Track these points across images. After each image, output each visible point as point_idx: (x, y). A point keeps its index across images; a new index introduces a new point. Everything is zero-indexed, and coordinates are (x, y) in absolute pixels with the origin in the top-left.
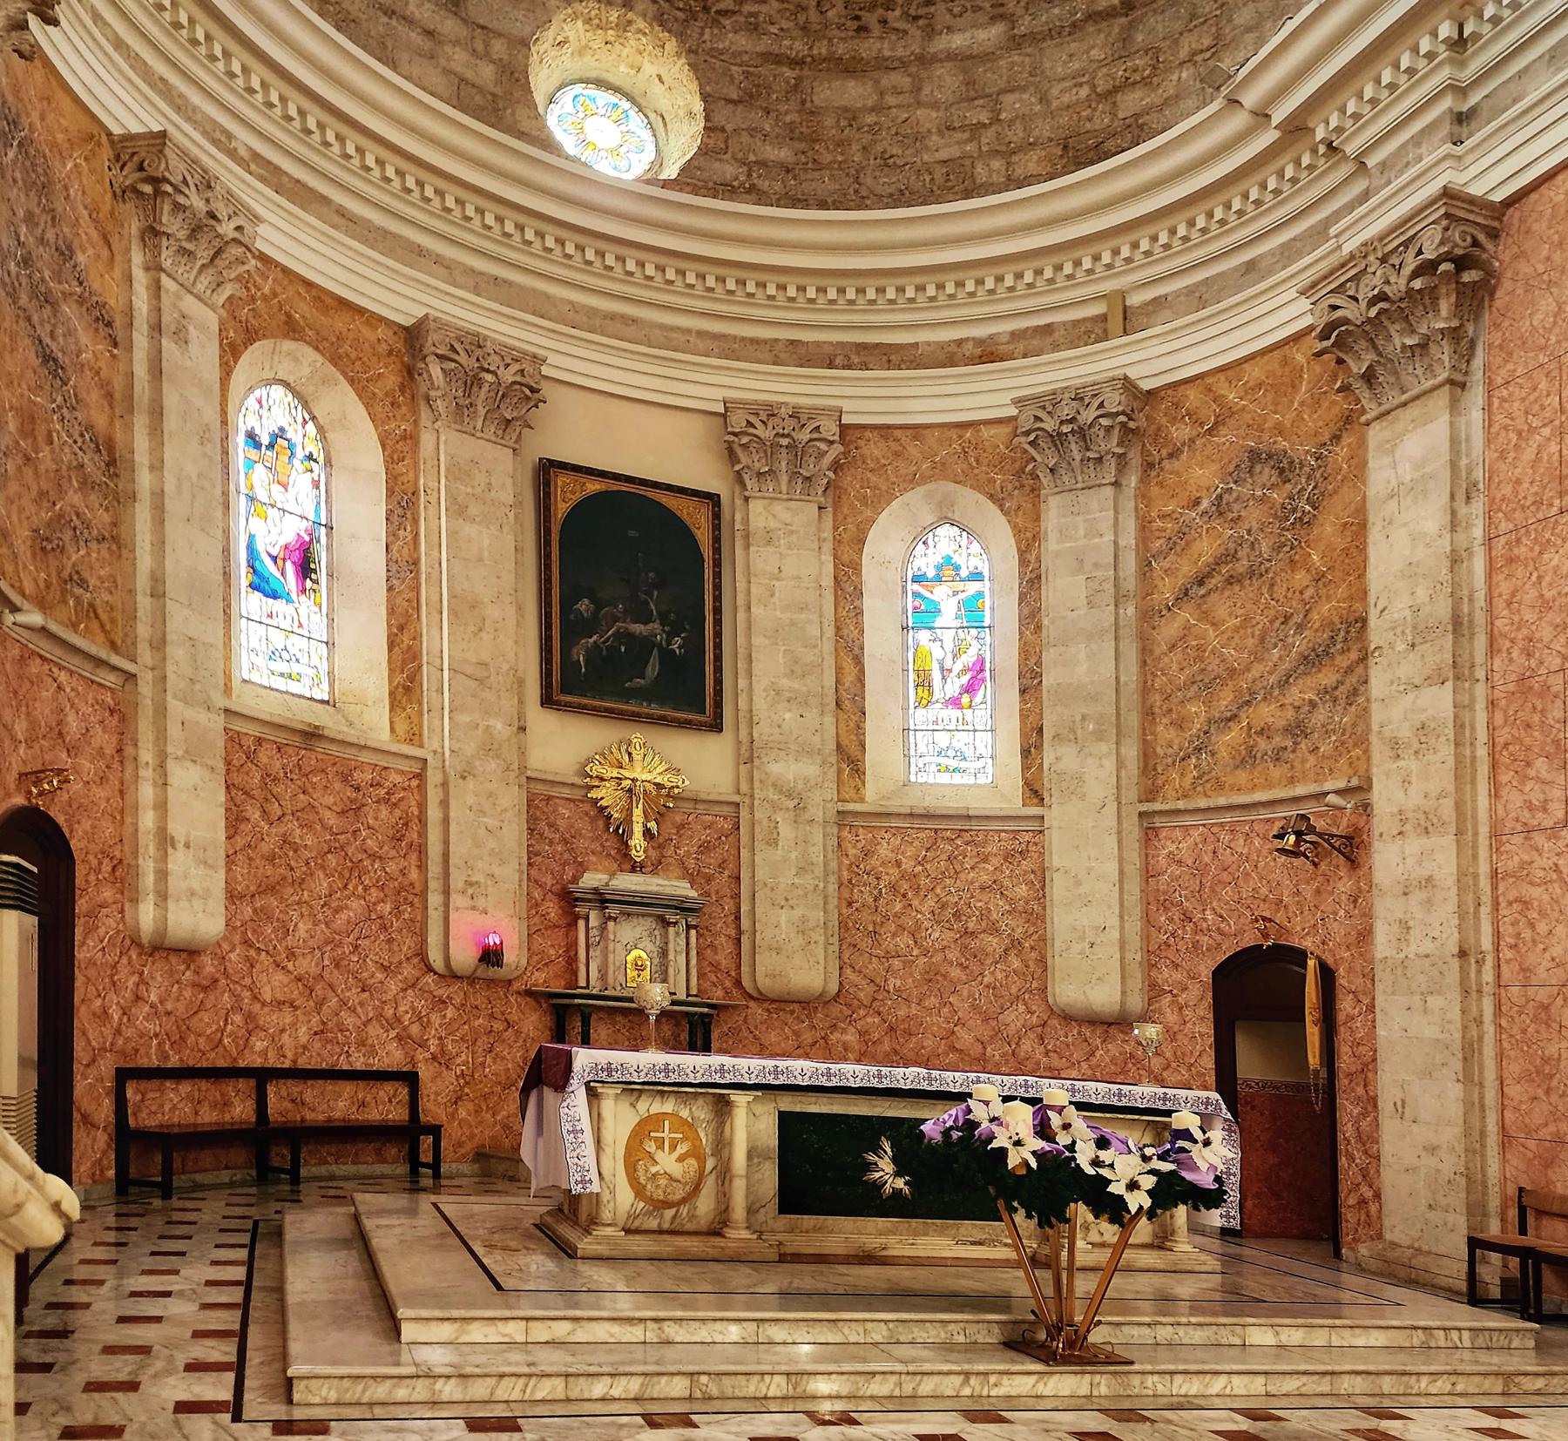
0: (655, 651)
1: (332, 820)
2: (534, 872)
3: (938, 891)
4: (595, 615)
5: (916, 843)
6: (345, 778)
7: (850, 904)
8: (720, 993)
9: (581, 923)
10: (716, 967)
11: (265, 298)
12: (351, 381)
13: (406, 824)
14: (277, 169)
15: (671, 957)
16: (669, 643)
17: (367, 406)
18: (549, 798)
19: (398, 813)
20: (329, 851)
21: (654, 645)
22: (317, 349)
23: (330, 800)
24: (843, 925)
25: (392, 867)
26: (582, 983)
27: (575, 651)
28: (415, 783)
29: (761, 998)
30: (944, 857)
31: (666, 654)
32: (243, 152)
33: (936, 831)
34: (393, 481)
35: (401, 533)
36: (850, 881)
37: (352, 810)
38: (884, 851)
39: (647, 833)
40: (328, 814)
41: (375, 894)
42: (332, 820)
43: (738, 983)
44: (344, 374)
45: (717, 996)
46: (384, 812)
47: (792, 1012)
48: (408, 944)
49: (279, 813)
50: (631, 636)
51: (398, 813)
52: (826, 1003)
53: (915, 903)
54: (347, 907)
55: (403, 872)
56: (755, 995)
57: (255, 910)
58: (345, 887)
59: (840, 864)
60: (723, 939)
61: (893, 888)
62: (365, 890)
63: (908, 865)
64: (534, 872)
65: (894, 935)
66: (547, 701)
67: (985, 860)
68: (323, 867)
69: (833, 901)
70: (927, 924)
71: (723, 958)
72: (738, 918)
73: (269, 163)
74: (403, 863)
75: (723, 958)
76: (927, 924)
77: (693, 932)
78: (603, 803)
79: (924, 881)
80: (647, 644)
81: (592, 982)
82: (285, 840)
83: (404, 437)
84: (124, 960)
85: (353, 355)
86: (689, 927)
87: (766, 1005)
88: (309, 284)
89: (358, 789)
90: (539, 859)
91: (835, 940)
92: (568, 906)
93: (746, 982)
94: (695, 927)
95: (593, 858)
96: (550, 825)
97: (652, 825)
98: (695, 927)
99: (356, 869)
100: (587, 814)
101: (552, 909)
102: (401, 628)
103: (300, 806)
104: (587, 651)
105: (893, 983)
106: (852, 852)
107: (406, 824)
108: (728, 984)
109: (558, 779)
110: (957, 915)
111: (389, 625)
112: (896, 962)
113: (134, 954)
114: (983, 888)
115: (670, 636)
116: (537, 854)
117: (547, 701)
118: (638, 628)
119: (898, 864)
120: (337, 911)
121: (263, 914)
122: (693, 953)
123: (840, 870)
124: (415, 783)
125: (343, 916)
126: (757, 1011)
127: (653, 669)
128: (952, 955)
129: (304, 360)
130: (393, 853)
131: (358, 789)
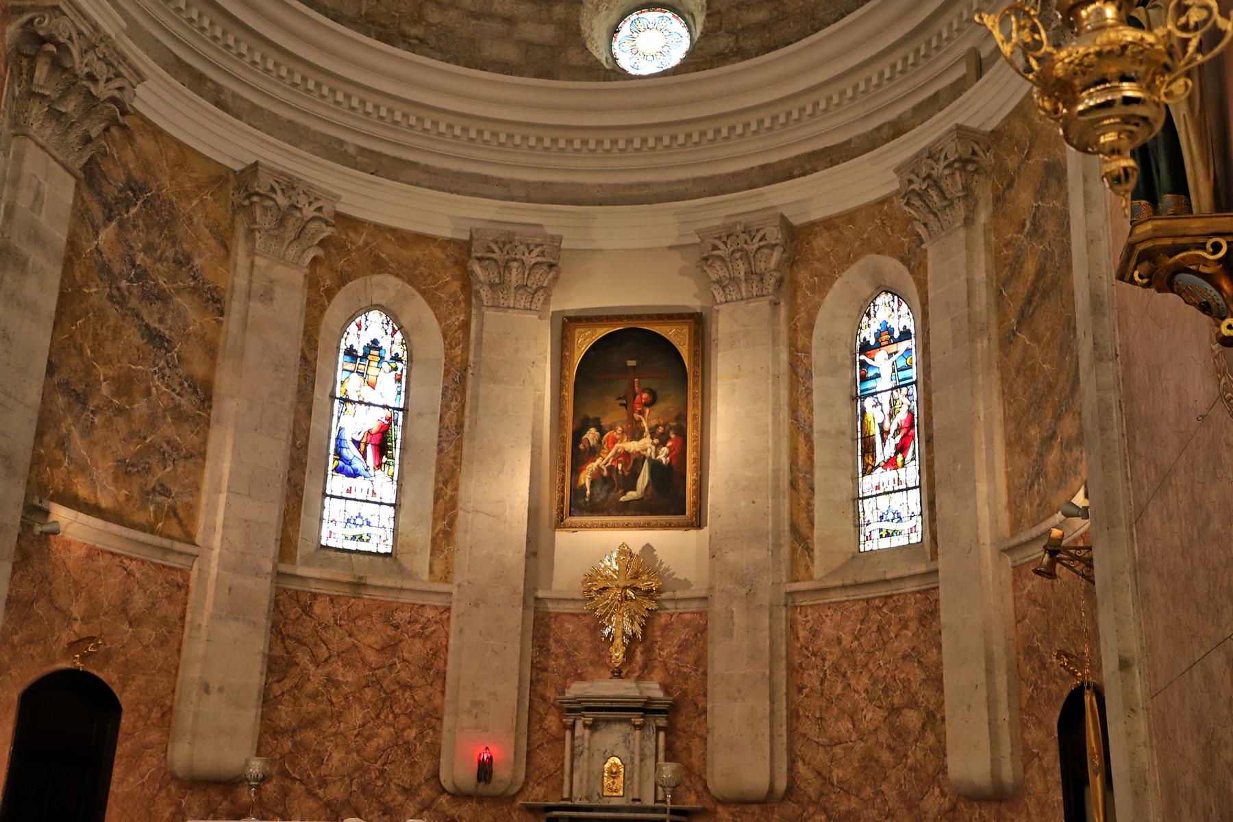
0: (646, 463)
1: (372, 657)
3: (871, 666)
4: (600, 442)
5: (853, 617)
6: (387, 620)
7: (800, 690)
11: (359, 249)
12: (423, 293)
13: (435, 654)
14: (380, 154)
16: (657, 455)
17: (434, 309)
19: (429, 644)
20: (367, 686)
21: (645, 457)
22: (397, 276)
23: (371, 639)
27: (582, 475)
28: (445, 616)
30: (875, 628)
31: (656, 466)
32: (351, 150)
33: (867, 601)
34: (449, 359)
35: (453, 404)
37: (390, 647)
38: (828, 629)
40: (369, 651)
41: (403, 720)
42: (372, 657)
44: (418, 290)
46: (418, 643)
48: (426, 766)
49: (326, 655)
50: (626, 454)
51: (429, 644)
53: (853, 682)
54: (377, 735)
57: (294, 744)
58: (378, 716)
61: (836, 667)
62: (395, 717)
63: (847, 639)
67: (905, 627)
68: (360, 700)
70: (862, 705)
73: (372, 151)
74: (430, 690)
76: (862, 705)
79: (860, 657)
80: (639, 459)
82: (331, 681)
83: (460, 327)
84: (163, 794)
85: (426, 272)
88: (394, 231)
89: (397, 627)
96: (556, 641)
99: (388, 699)
102: (446, 483)
103: (344, 648)
104: (593, 474)
105: (837, 774)
106: (802, 634)
107: (435, 654)
109: (561, 596)
110: (885, 691)
111: (437, 481)
112: (838, 750)
113: (173, 788)
114: (904, 657)
115: (657, 446)
118: (633, 446)
119: (839, 640)
120: (368, 740)
121: (299, 747)
125: (373, 744)
127: (644, 479)
128: (883, 736)
129: (389, 285)
130: (422, 682)
131: (397, 627)
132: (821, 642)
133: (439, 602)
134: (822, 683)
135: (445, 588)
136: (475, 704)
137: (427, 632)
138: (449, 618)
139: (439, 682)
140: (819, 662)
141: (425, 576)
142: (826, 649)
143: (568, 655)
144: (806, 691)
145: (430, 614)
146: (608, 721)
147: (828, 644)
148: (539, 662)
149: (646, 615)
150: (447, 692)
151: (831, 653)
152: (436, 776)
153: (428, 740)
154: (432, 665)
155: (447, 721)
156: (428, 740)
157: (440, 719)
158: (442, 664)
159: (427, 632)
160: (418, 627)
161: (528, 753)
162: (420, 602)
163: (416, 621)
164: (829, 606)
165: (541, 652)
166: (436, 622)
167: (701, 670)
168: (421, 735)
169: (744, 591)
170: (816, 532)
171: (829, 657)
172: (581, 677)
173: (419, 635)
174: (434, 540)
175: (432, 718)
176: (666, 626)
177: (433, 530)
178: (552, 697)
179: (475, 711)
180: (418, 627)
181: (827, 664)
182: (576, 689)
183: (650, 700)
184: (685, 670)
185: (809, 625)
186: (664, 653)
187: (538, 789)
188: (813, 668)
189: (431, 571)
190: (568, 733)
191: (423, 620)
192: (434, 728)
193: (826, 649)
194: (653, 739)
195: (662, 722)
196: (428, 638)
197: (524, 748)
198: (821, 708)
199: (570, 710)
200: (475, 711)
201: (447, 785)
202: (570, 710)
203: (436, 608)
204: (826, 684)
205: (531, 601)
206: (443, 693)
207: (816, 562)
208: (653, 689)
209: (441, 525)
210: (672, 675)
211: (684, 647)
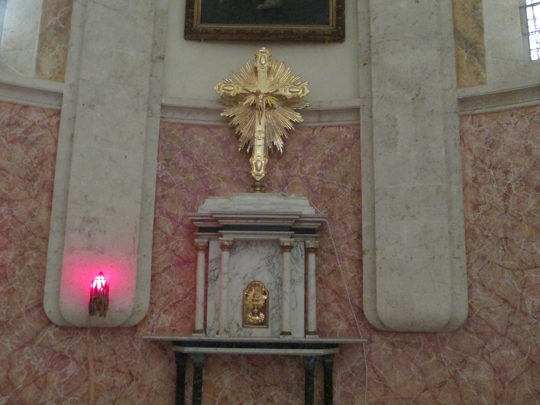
2: (166, 205)
7: (476, 207)
8: (342, 326)
9: (201, 256)
10: (339, 295)
13: (41, 164)
15: (287, 288)
18: (186, 127)
19: (34, 151)
24: (470, 234)
25: (20, 210)
26: (199, 326)
28: (54, 121)
29: (383, 331)
36: (475, 179)
38: (511, 138)
39: (272, 152)
43: (360, 312)
45: (340, 331)
46: (19, 151)
47: (418, 345)
51: (34, 151)
52: (455, 332)
55: (32, 215)
56: (383, 329)
59: (464, 160)
60: (347, 262)
64: (166, 205)
65: (529, 240)
66: (191, 34)
69: (458, 205)
71: (345, 283)
72: (360, 237)
75: (345, 283)
77: (312, 257)
78: (235, 121)
81: (209, 324)
86: (308, 251)
87: (390, 338)
90: (173, 190)
91: (461, 253)
92: (193, 238)
93: (368, 313)
94: (315, 250)
95: (224, 185)
97: (279, 143)
98: (315, 250)
100: (220, 139)
101: (180, 244)
106: (475, 145)
107: (41, 164)
108: (352, 314)
116: (171, 185)
117: (191, 34)
122: (312, 281)
123: (464, 169)
124: (54, 121)
126: (381, 347)
130: (24, 194)
132: (501, 153)
133: (49, 103)
134: (505, 197)
135: (54, 86)
136: (88, 220)
137: (31, 138)
138: (58, 123)
139: (45, 196)
140: (499, 174)
141: (32, 73)
142: (509, 160)
143: (199, 169)
144: (483, 208)
145: (34, 116)
146: (247, 243)
147: (511, 154)
148: (166, 177)
149: (290, 126)
150: (54, 207)
151: (517, 165)
152: (40, 305)
153: (31, 263)
154: (38, 175)
155: (54, 241)
156: (31, 263)
157: (46, 239)
158: (49, 175)
159: (31, 138)
160: (19, 131)
161: (153, 277)
162: (25, 103)
163: (17, 124)
164: (512, 112)
165: (167, 166)
166: (43, 127)
167: (349, 187)
168: (22, 257)
169: (409, 97)
170: (486, 37)
171: (514, 170)
172: (212, 193)
173: (23, 141)
174: (43, 35)
175: (37, 239)
176: (308, 141)
177: (43, 23)
178: (181, 214)
179: (87, 229)
180: (19, 131)
181: (511, 178)
182: (211, 206)
183: (300, 218)
184: (329, 187)
185: (483, 136)
186: (306, 169)
187: (163, 316)
188: (491, 182)
189: (38, 69)
190: (201, 256)
191: (27, 123)
192: (37, 249)
193: (509, 160)
194: (302, 261)
195: (311, 243)
196: (32, 144)
197: (147, 273)
198: (505, 227)
199: (202, 230)
200: (87, 229)
201: (53, 316)
202: (202, 230)
203: (43, 110)
204: (512, 200)
205: (157, 108)
206: (50, 208)
207: (489, 68)
208: (299, 205)
209: (52, 20)
210: (316, 192)
211: (329, 162)
